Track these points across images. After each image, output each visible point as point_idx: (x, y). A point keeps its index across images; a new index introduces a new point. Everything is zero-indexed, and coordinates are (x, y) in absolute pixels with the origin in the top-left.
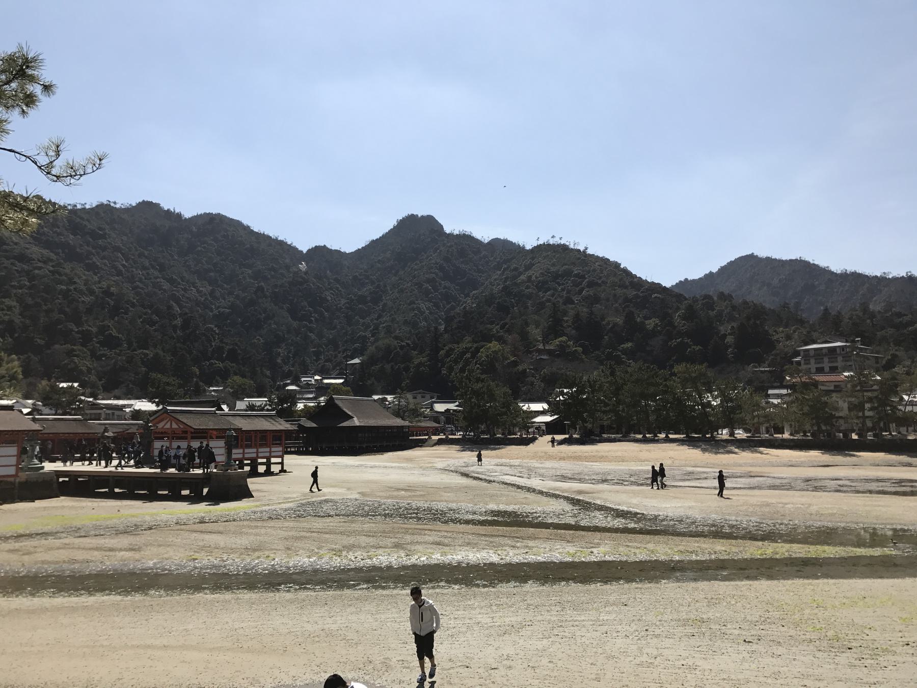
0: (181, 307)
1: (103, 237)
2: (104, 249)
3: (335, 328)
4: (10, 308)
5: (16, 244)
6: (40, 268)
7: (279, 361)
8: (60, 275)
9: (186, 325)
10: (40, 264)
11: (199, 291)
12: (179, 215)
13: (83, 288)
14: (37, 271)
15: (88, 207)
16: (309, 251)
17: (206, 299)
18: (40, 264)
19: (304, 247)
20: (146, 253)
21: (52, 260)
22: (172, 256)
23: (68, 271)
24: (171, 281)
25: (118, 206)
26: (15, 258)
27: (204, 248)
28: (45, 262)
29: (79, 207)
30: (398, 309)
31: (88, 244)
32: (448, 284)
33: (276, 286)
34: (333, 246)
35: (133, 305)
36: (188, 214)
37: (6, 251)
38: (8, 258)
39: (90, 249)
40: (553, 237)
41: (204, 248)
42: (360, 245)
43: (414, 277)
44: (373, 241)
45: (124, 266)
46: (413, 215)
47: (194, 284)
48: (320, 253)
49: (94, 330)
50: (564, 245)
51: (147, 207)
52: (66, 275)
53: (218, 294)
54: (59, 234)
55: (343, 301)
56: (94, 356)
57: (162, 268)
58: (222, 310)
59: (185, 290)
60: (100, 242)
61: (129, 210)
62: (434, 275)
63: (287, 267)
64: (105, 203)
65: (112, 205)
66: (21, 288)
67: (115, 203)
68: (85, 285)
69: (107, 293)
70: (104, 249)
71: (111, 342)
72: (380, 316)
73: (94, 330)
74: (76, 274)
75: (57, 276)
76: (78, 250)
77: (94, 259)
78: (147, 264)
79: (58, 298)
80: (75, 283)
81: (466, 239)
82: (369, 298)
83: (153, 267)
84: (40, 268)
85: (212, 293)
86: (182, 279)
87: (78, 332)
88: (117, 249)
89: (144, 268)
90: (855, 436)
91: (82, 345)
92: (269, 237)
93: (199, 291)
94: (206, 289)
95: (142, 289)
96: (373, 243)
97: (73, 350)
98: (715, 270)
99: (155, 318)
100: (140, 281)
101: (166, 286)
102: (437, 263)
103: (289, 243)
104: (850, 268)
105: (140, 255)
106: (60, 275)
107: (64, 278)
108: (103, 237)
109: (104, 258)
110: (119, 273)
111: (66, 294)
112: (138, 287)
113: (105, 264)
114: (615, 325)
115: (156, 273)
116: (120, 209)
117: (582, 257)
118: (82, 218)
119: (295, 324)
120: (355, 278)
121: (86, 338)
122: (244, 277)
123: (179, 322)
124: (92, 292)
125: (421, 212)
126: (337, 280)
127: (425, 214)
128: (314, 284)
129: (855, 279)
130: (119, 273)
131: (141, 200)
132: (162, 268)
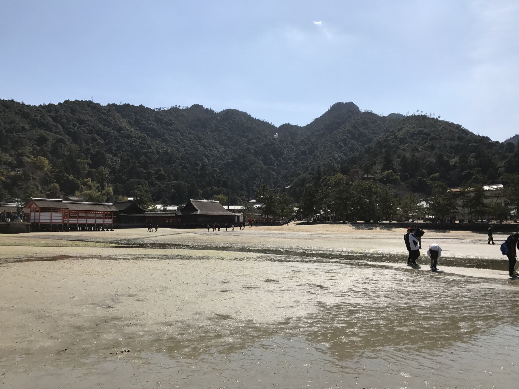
0: (208, 159)
1: (171, 124)
2: (171, 130)
3: (287, 169)
4: (116, 161)
5: (127, 130)
6: (135, 142)
7: (254, 187)
8: (144, 144)
9: (203, 167)
10: (136, 140)
11: (218, 151)
12: (212, 111)
14: (134, 143)
15: (166, 109)
17: (221, 155)
18: (136, 140)
19: (277, 125)
20: (192, 132)
21: (142, 137)
22: (207, 133)
23: (149, 142)
24: (204, 146)
25: (181, 108)
26: (125, 137)
28: (139, 139)
29: (162, 109)
30: (322, 158)
31: (164, 128)
32: (353, 142)
33: (257, 147)
34: (293, 123)
35: (178, 159)
37: (122, 134)
38: (122, 137)
39: (164, 131)
40: (418, 111)
42: (309, 121)
43: (334, 138)
44: (316, 119)
45: (181, 139)
46: (340, 102)
48: (286, 127)
49: (153, 172)
50: (425, 116)
51: (196, 107)
52: (147, 144)
53: (228, 152)
54: (150, 124)
55: (293, 154)
56: (151, 184)
57: (200, 139)
58: (228, 161)
59: (211, 151)
61: (186, 110)
62: (345, 137)
63: (266, 137)
66: (126, 151)
68: (156, 149)
69: (166, 153)
70: (171, 130)
71: (160, 178)
72: (312, 162)
73: (153, 172)
74: (152, 144)
76: (159, 132)
78: (192, 138)
80: (151, 148)
81: (369, 115)
82: (307, 152)
84: (135, 142)
85: (225, 152)
86: (210, 145)
87: (145, 173)
88: (178, 130)
89: (191, 140)
90: (457, 222)
91: (146, 179)
92: (258, 120)
93: (218, 151)
94: (222, 149)
95: (189, 150)
96: (317, 120)
97: (140, 182)
99: (188, 165)
100: (189, 147)
101: (201, 148)
102: (348, 130)
103: (270, 123)
105: (189, 134)
106: (144, 144)
108: (171, 124)
109: (171, 135)
110: (178, 143)
111: (146, 154)
112: (187, 150)
113: (171, 138)
114: (431, 162)
115: (197, 142)
117: (435, 122)
118: (161, 115)
119: (265, 167)
120: (302, 140)
121: (149, 175)
123: (199, 167)
124: (158, 153)
125: (345, 100)
126: (292, 143)
127: (348, 101)
128: (277, 145)
130: (178, 143)
132: (200, 139)
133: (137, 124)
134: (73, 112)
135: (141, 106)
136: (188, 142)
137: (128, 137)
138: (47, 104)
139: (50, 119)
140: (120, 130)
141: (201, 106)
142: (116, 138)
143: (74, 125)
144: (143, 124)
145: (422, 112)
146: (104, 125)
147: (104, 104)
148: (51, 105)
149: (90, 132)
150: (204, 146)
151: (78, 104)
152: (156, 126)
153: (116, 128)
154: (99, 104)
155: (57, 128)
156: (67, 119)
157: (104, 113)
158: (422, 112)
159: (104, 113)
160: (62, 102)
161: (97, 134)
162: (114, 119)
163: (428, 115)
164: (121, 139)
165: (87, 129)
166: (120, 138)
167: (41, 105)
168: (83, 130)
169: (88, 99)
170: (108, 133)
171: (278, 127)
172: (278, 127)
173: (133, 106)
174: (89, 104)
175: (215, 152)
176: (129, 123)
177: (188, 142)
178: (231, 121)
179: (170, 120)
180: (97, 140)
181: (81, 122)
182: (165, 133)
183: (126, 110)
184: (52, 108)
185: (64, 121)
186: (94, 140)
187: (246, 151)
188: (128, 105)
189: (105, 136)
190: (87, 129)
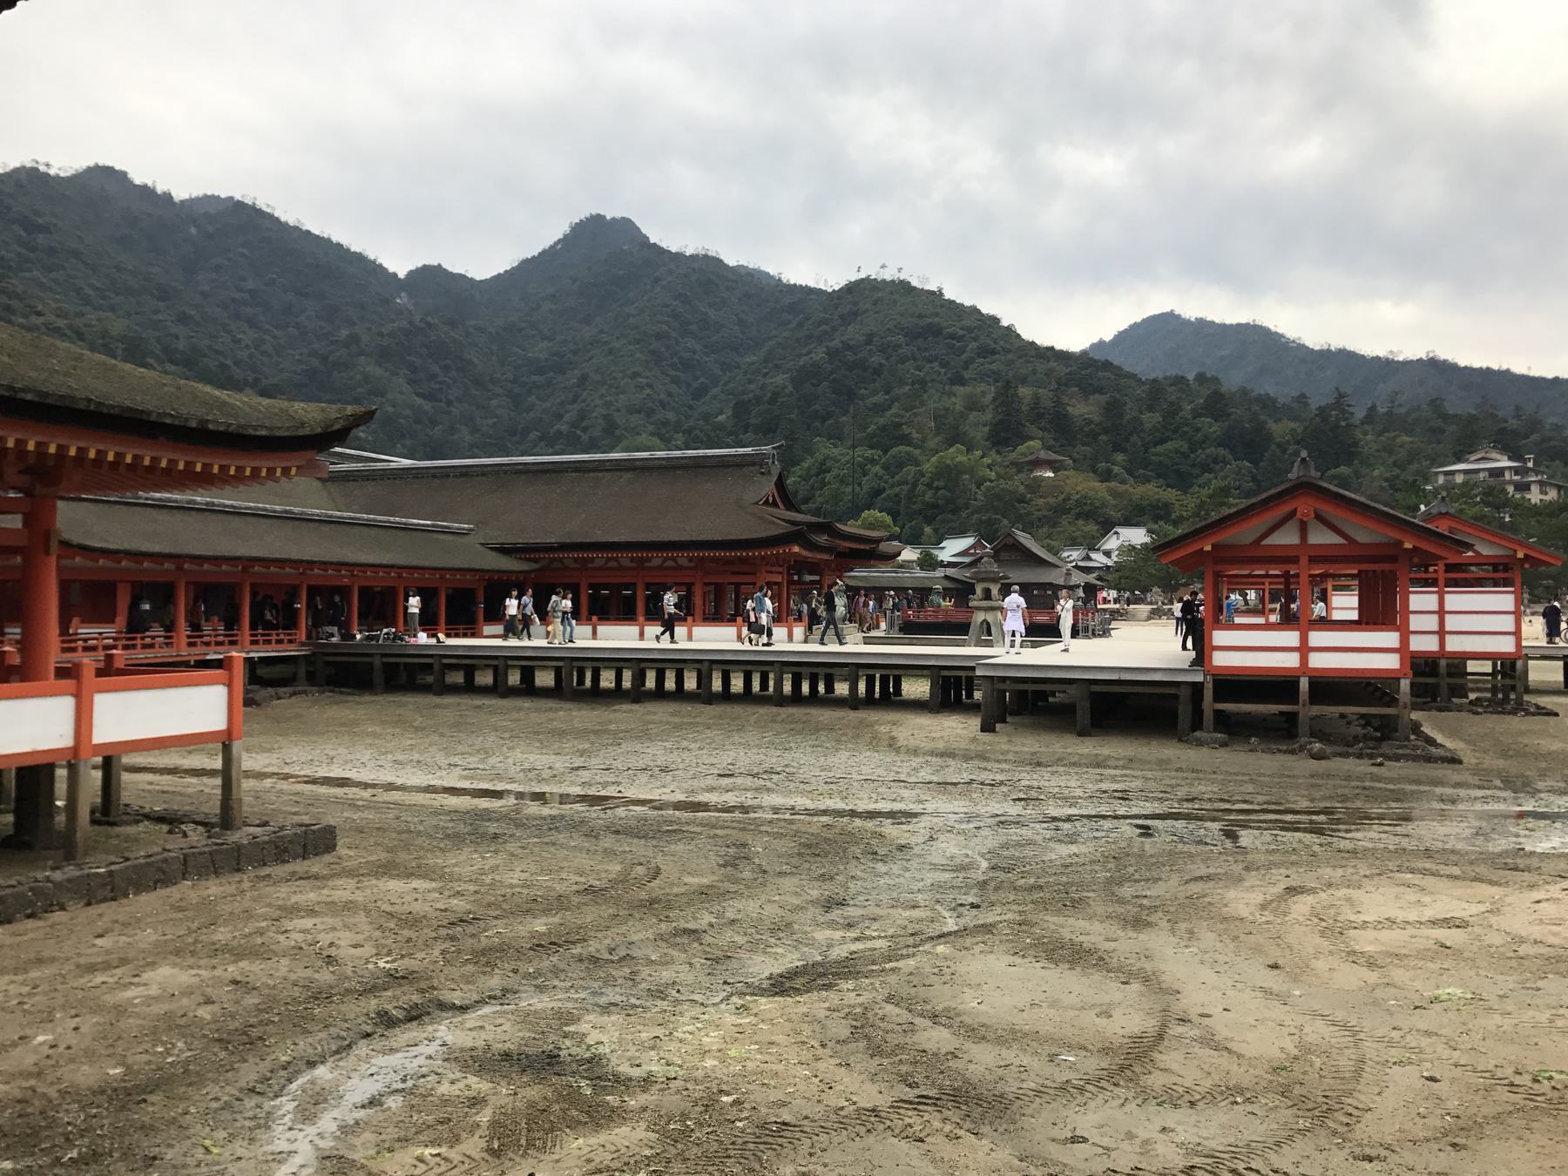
12: (167, 197)
16: (411, 273)
25: (52, 172)
33: (380, 334)
36: (180, 194)
48: (429, 277)
60: (41, 239)
64: (29, 165)
65: (42, 168)
93: (239, 341)
96: (526, 264)
98: (1108, 338)
104: (1336, 343)
116: (57, 177)
119: (427, 406)
127: (618, 215)
129: (1345, 360)
131: (92, 164)
141: (124, 174)
145: (900, 270)
150: (183, 319)
158: (900, 270)
163: (915, 283)
171: (401, 275)
172: (401, 275)
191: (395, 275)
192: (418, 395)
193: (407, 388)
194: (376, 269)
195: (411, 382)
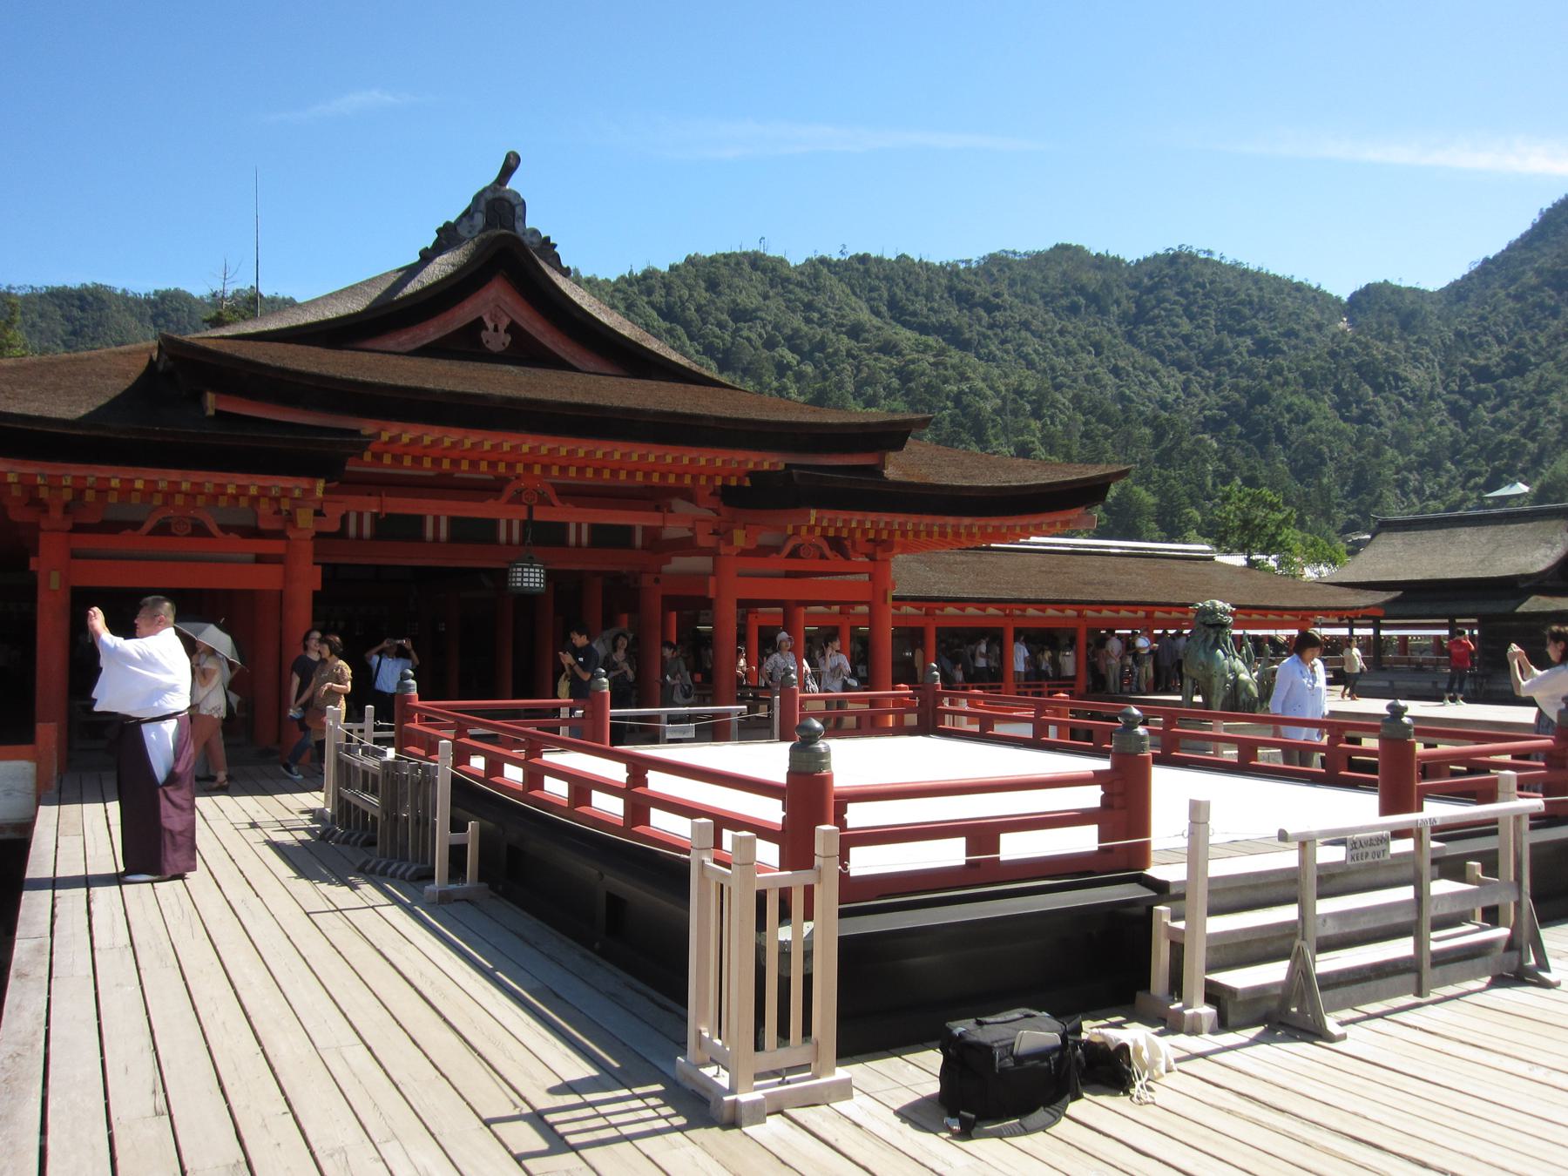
2: (1006, 326)
5: (879, 329)
12: (1117, 261)
13: (980, 385)
24: (1116, 371)
26: (880, 350)
27: (1165, 310)
38: (868, 351)
41: (1165, 310)
44: (1486, 261)
47: (1154, 373)
51: (1063, 252)
52: (954, 367)
63: (1319, 327)
67: (1014, 253)
75: (942, 371)
77: (993, 348)
79: (945, 408)
80: (968, 379)
83: (1083, 348)
92: (1275, 277)
94: (1174, 379)
101: (1109, 379)
107: (950, 372)
109: (1003, 342)
111: (957, 399)
113: (1007, 352)
119: (1351, 429)
122: (1240, 354)
133: (898, 312)
134: (713, 286)
135: (902, 258)
136: (1059, 361)
137: (888, 348)
138: (638, 272)
139: (655, 314)
140: (855, 332)
141: (1079, 250)
142: (849, 354)
143: (721, 326)
144: (914, 314)
146: (808, 321)
147: (796, 259)
148: (649, 274)
149: (770, 344)
151: (726, 264)
152: (953, 315)
153: (842, 325)
154: (782, 261)
155: (672, 336)
156: (699, 309)
157: (801, 285)
159: (801, 285)
160: (679, 260)
161: (794, 349)
162: (832, 298)
164: (868, 359)
165: (760, 336)
166: (865, 356)
167: (623, 277)
168: (749, 339)
169: (751, 246)
170: (821, 345)
172: (1345, 298)
173: (879, 260)
174: (756, 261)
175: (1154, 389)
176: (877, 313)
177: (1059, 361)
178: (1189, 286)
179: (997, 295)
180: (789, 366)
181: (740, 315)
182: (986, 337)
183: (861, 271)
184: (653, 282)
185: (691, 313)
186: (782, 368)
187: (1269, 377)
188: (864, 259)
189: (812, 351)
190: (760, 336)
191: (1338, 299)
192: (1346, 419)
193: (1332, 413)
194: (1317, 297)
195: (1337, 407)
